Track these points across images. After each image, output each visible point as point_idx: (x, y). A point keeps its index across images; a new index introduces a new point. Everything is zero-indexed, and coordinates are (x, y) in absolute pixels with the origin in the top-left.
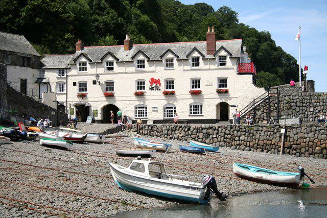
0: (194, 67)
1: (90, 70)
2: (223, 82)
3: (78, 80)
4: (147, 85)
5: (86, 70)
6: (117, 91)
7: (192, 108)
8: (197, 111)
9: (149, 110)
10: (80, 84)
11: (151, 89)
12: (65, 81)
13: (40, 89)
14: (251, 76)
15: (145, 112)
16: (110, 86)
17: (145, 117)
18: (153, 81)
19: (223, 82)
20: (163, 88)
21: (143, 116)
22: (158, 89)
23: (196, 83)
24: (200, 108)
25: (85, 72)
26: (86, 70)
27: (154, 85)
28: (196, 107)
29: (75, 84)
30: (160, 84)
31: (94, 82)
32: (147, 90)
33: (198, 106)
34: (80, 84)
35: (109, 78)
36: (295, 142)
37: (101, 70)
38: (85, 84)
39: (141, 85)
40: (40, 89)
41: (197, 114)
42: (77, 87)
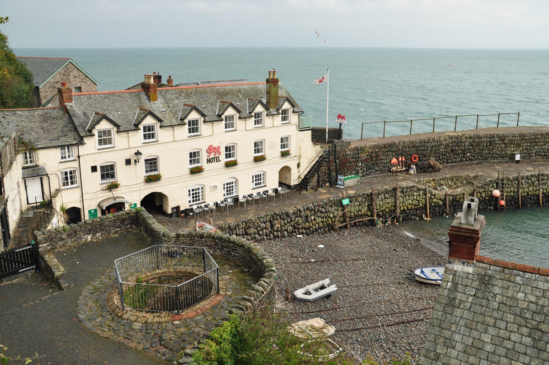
0: (257, 126)
1: (119, 140)
2: (284, 142)
3: (102, 160)
4: (204, 157)
5: (110, 143)
6: (163, 169)
7: (254, 179)
8: (259, 181)
9: (207, 190)
10: (102, 168)
11: (209, 161)
12: (75, 164)
13: (26, 187)
14: (310, 131)
15: (201, 194)
16: (152, 163)
17: (201, 201)
18: (210, 149)
19: (284, 142)
20: (223, 159)
21: (199, 200)
22: (217, 160)
23: (258, 146)
24: (262, 177)
25: (108, 146)
26: (110, 143)
27: (212, 156)
28: (258, 177)
29: (94, 169)
30: (220, 153)
31: (128, 162)
32: (203, 163)
33: (261, 175)
34: (102, 168)
35: (148, 152)
36: (381, 209)
37: (138, 137)
38: (112, 167)
39: (194, 156)
40: (26, 187)
41: (260, 186)
42: (99, 173)
